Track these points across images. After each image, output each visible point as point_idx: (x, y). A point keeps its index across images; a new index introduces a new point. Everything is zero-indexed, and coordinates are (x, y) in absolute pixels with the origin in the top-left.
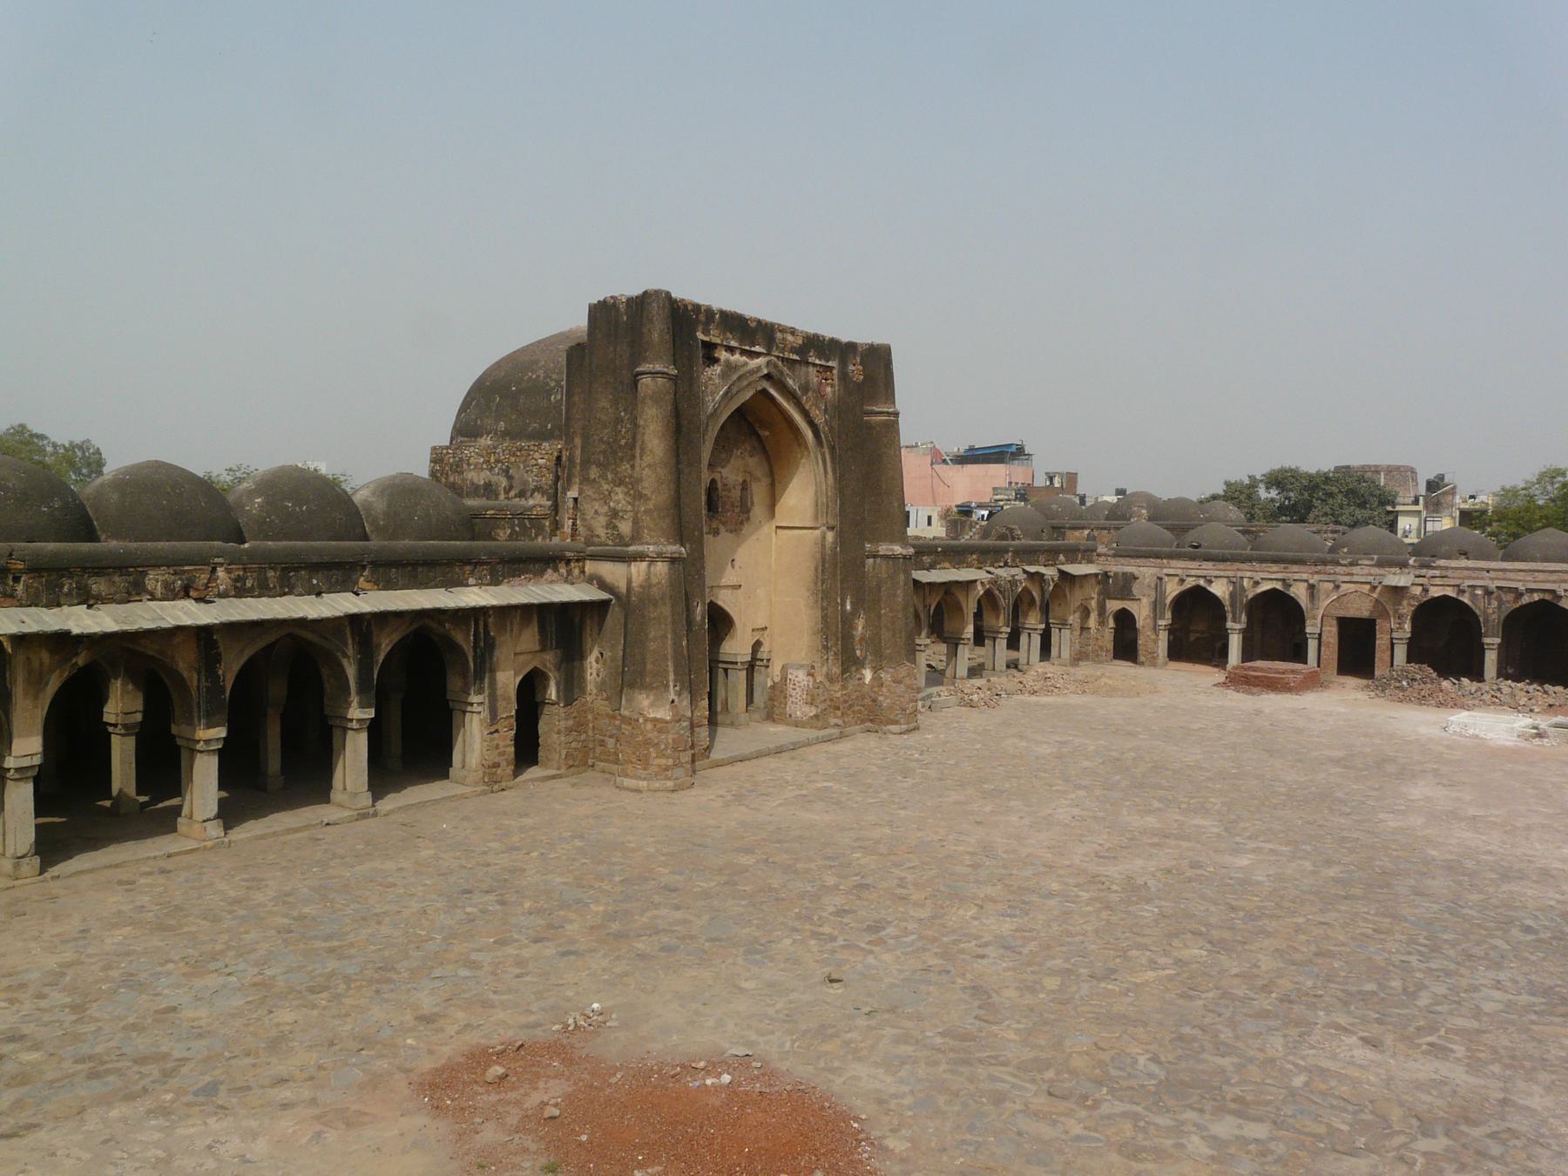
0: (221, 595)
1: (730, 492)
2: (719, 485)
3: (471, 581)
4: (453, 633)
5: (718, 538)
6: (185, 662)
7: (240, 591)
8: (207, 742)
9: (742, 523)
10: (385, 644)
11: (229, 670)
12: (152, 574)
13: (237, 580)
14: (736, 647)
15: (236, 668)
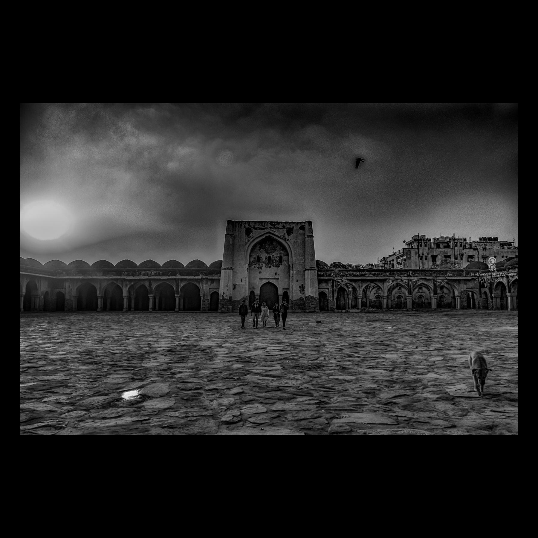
0: (153, 276)
1: (275, 258)
2: (271, 257)
3: (201, 275)
4: (196, 284)
5: (270, 268)
6: (147, 284)
7: (155, 275)
8: (150, 296)
9: (279, 265)
10: (182, 285)
11: (154, 286)
12: (142, 272)
13: (155, 273)
14: (280, 292)
15: (155, 286)
